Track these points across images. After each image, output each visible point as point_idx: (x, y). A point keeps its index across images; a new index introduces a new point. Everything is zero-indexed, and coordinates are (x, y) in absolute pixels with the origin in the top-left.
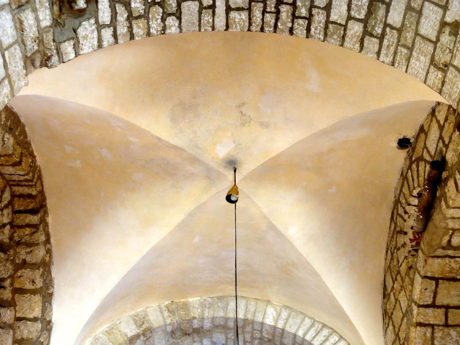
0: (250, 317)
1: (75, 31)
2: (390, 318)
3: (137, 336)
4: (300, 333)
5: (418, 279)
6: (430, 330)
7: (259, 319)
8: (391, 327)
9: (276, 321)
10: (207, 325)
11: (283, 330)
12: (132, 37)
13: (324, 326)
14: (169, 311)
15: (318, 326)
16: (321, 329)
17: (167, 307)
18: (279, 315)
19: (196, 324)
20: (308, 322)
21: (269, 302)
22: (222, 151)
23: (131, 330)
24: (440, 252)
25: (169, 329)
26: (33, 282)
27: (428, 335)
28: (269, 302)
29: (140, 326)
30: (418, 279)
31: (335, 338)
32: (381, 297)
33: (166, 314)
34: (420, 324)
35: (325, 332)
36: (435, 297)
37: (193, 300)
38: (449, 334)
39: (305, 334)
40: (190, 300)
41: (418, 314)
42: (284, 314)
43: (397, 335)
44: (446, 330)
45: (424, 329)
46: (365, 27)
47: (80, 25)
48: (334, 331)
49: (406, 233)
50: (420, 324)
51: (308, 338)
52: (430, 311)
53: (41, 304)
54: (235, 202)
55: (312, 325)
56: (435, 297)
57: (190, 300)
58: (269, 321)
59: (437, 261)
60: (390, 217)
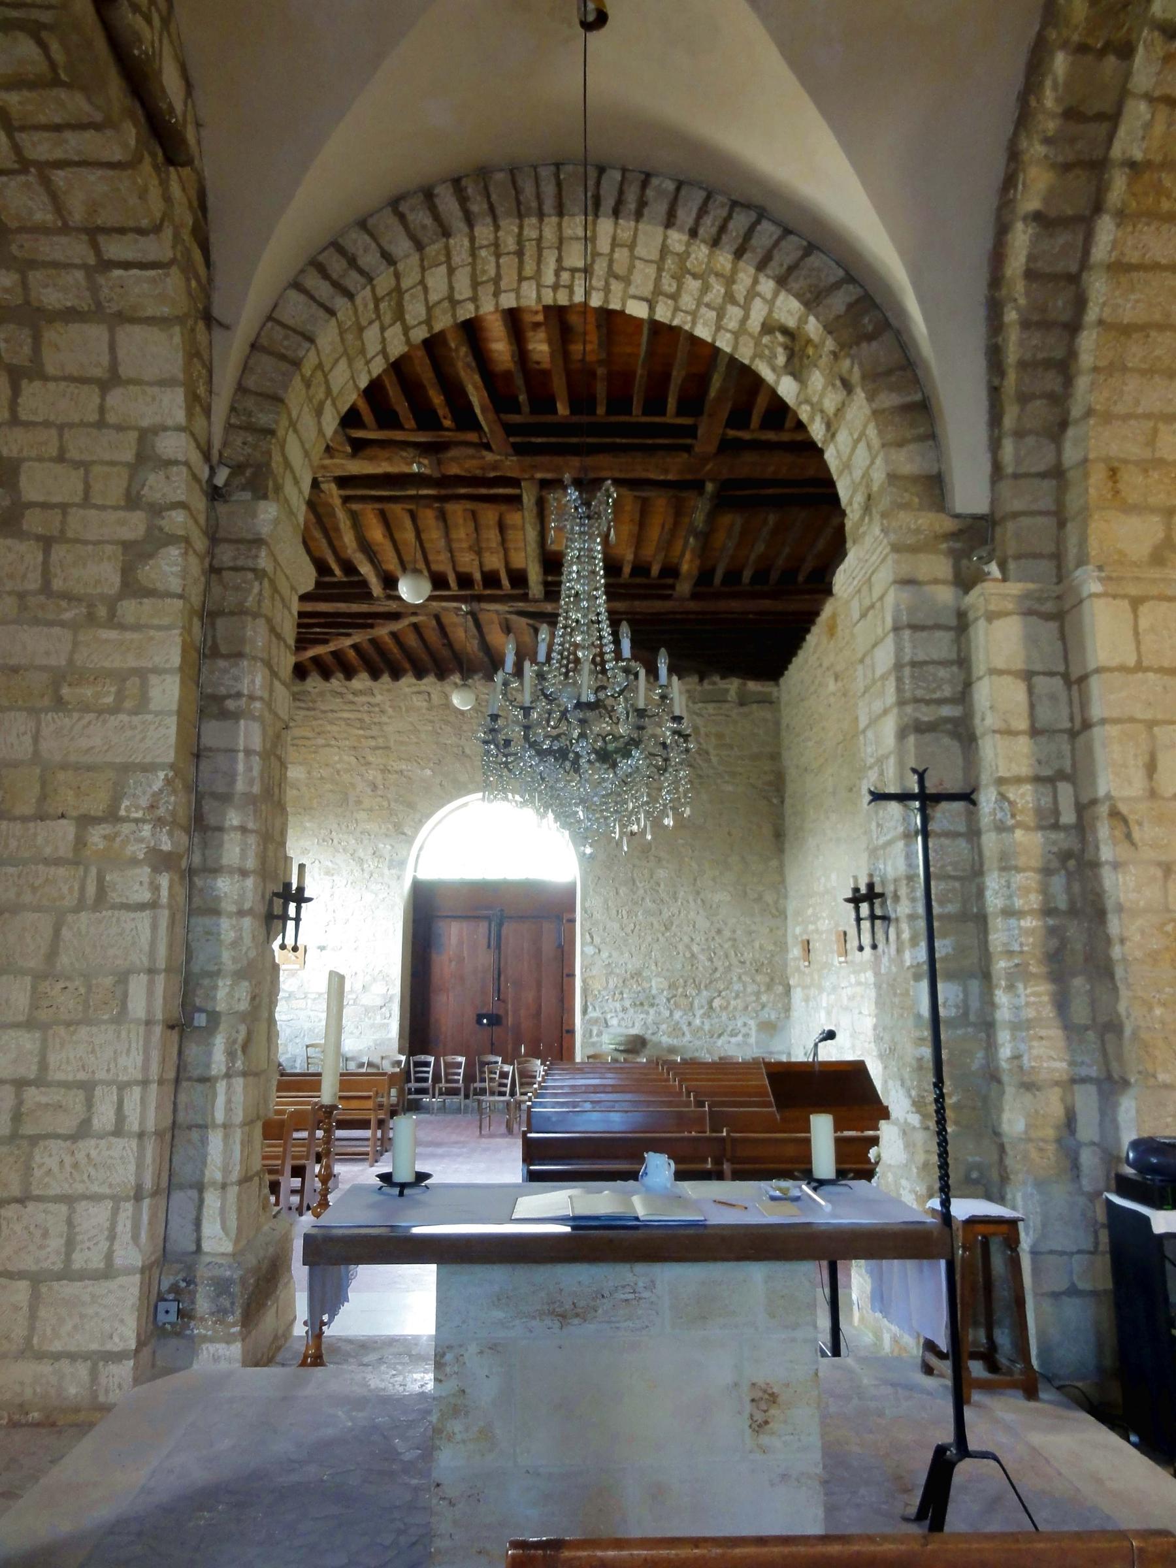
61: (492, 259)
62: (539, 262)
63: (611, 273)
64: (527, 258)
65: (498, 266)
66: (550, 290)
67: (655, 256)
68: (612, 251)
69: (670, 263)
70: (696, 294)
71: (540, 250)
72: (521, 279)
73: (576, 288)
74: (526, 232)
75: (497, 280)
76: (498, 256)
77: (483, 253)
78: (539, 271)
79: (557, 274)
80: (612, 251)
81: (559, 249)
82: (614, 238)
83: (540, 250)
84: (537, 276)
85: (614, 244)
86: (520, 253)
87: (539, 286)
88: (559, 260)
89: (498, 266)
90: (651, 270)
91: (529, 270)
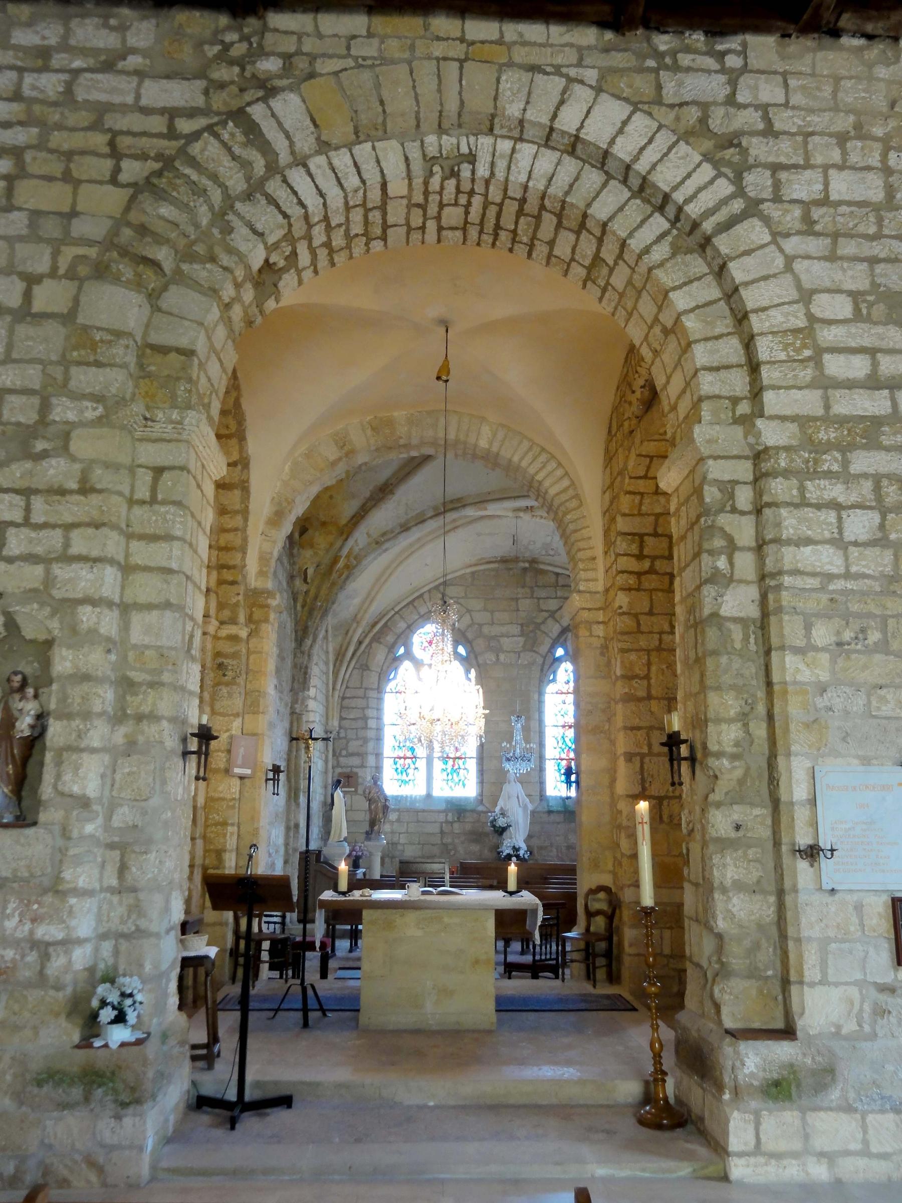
0: (462, 437)
1: (275, 285)
2: (611, 459)
3: (340, 459)
4: (516, 459)
5: (633, 456)
6: (638, 497)
7: (472, 440)
8: (608, 469)
9: (491, 443)
10: (415, 441)
11: (498, 454)
12: (333, 264)
13: (543, 449)
14: (373, 429)
15: (536, 450)
16: (540, 454)
17: (369, 423)
18: (494, 435)
19: (402, 442)
20: (526, 444)
21: (483, 419)
22: (434, 312)
23: (332, 453)
24: (657, 437)
25: (373, 448)
26: (227, 427)
27: (637, 501)
28: (483, 419)
29: (342, 447)
30: (633, 456)
31: (554, 465)
32: (606, 431)
33: (369, 432)
34: (630, 493)
35: (543, 457)
36: (647, 471)
37: (399, 415)
38: (658, 501)
39: (522, 459)
40: (396, 414)
41: (629, 484)
42: (500, 435)
43: (612, 483)
44: (655, 497)
45: (632, 497)
46: (589, 273)
47: (280, 278)
48: (553, 457)
49: (633, 392)
50: (630, 493)
51: (524, 464)
52: (641, 482)
53: (237, 447)
54: (447, 381)
55: (530, 449)
56: (647, 471)
57: (396, 414)
58: (483, 444)
59: (652, 443)
60: (624, 356)
61: (519, 232)
62: (484, 215)
63: (423, 207)
64: (493, 221)
65: (516, 223)
66: (477, 190)
67: (390, 231)
68: (424, 223)
69: (378, 231)
70: (352, 226)
71: (482, 224)
72: (501, 205)
73: (454, 190)
74: (491, 241)
75: (520, 213)
76: (514, 232)
77: (525, 239)
78: (485, 208)
79: (469, 204)
80: (424, 223)
81: (466, 222)
82: (424, 233)
83: (482, 224)
84: (486, 205)
85: (423, 228)
86: (498, 227)
87: (486, 196)
88: (467, 213)
89: (516, 223)
90: (391, 220)
91: (492, 211)
